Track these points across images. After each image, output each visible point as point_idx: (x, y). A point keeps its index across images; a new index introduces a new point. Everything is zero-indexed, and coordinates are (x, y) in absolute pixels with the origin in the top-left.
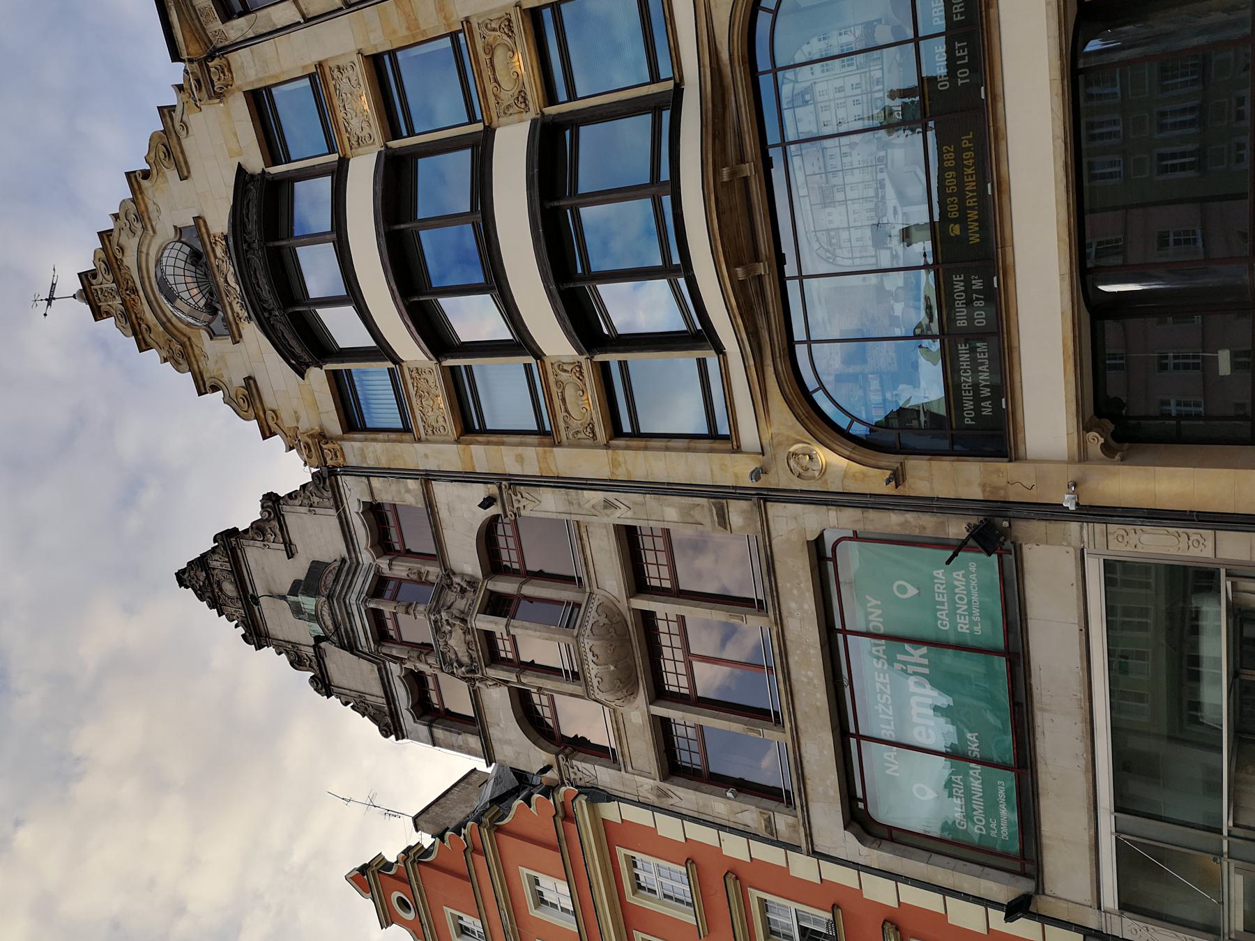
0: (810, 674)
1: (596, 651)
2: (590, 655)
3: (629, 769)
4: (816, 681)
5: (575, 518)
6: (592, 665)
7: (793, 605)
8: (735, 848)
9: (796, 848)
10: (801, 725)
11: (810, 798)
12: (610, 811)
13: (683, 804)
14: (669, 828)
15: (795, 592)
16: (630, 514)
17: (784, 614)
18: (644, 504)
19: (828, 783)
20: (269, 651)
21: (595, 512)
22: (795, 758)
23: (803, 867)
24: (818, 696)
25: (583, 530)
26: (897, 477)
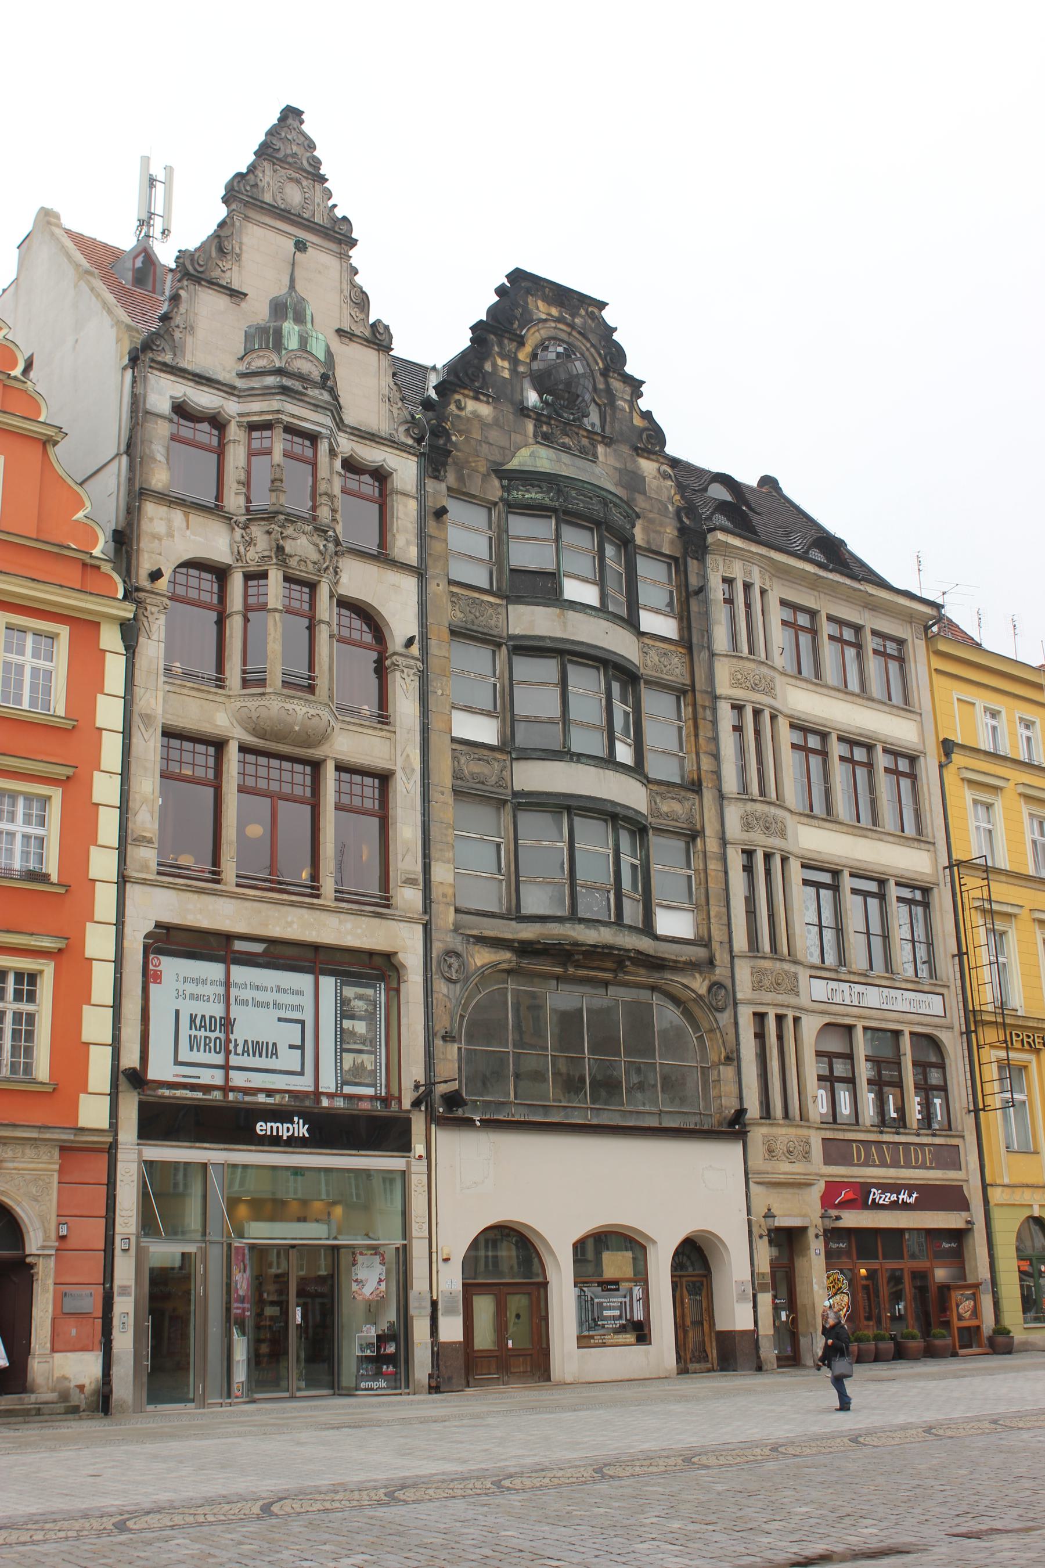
0: (295, 926)
1: (316, 719)
2: (312, 712)
4: (289, 929)
6: (304, 710)
7: (349, 926)
8: (105, 789)
10: (248, 904)
11: (180, 892)
14: (109, 712)
15: (359, 931)
17: (342, 916)
19: (199, 917)
20: (221, 212)
22: (221, 891)
23: (103, 864)
24: (278, 929)
25: (388, 734)
26: (448, 1038)
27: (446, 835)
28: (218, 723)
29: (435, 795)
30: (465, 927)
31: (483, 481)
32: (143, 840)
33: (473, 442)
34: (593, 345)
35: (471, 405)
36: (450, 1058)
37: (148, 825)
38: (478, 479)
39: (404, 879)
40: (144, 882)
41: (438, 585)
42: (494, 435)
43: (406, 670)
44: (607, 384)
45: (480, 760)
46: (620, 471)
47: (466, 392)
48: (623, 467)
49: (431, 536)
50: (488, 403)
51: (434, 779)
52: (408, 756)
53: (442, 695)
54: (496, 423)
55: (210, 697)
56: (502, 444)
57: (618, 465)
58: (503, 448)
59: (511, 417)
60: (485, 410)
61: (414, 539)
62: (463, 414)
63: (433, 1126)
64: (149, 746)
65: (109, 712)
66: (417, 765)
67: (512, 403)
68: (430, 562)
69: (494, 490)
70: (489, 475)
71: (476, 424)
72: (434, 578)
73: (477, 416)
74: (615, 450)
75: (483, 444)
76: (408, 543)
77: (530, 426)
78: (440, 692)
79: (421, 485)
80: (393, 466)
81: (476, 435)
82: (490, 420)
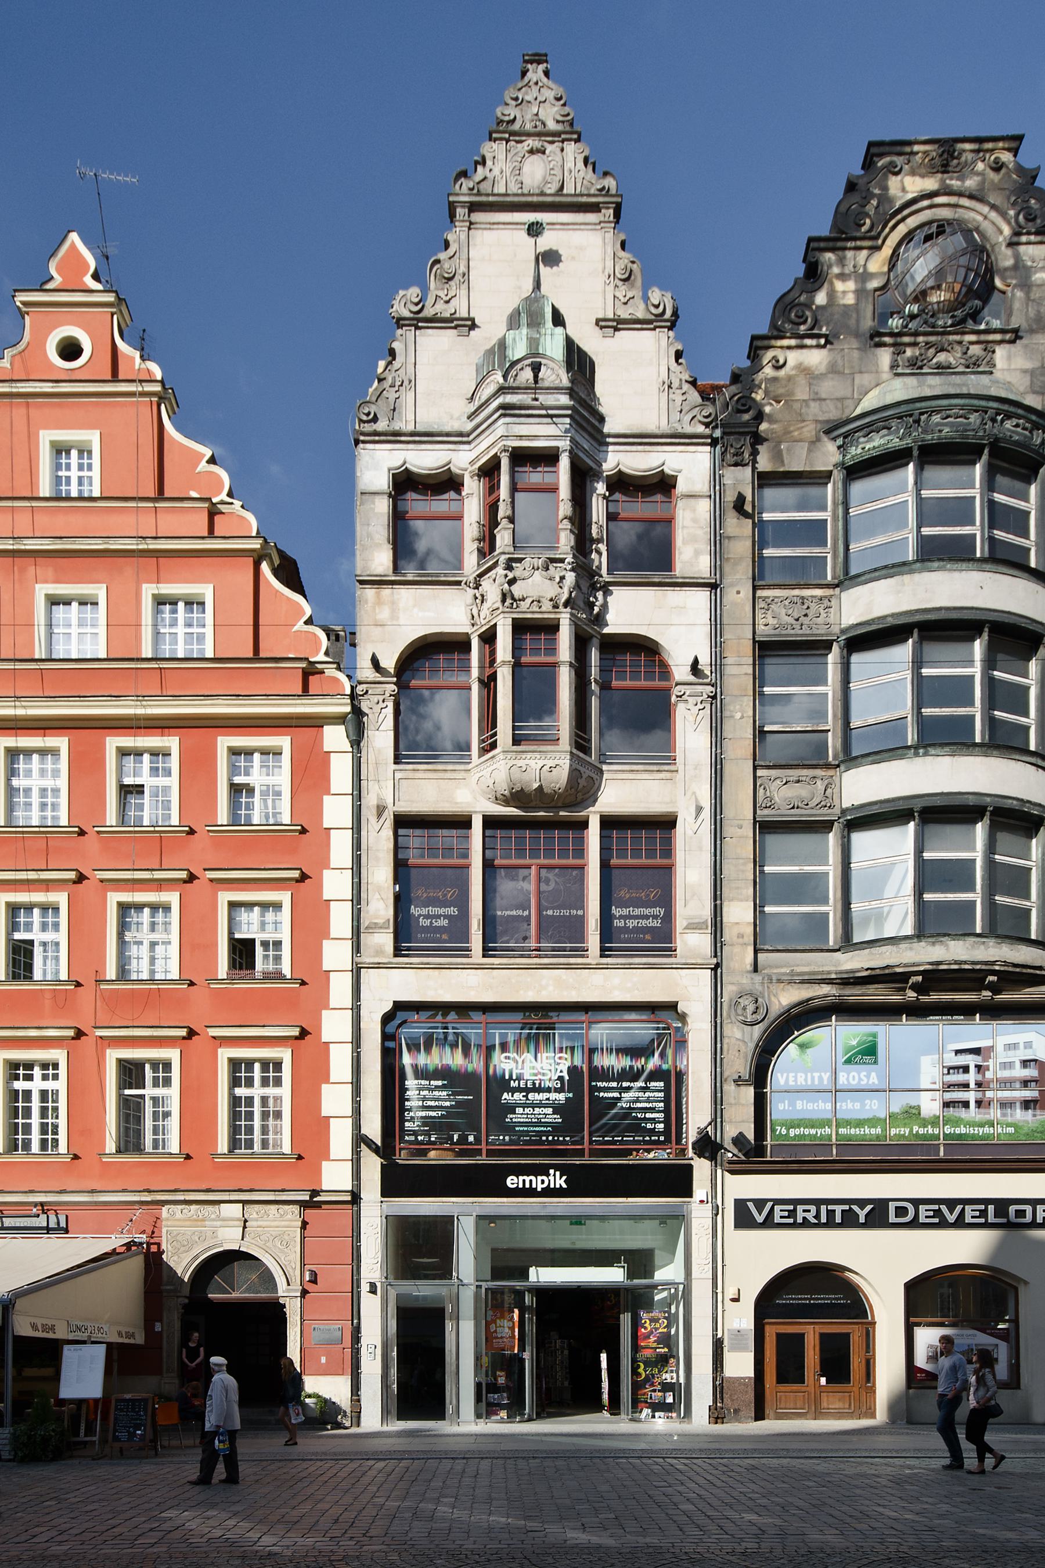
0: (551, 988)
3: (398, 775)
5: (681, 768)
8: (336, 884)
9: (357, 948)
12: (335, 737)
13: (373, 834)
14: (336, 811)
16: (690, 833)
18: (700, 849)
21: (689, 794)
23: (336, 955)
25: (668, 775)
27: (743, 871)
28: (459, 800)
29: (729, 830)
30: (770, 967)
31: (809, 451)
32: (374, 927)
33: (796, 406)
34: (993, 207)
35: (793, 358)
36: (743, 1102)
37: (382, 913)
38: (802, 450)
39: (685, 924)
40: (378, 966)
41: (738, 592)
42: (828, 387)
43: (690, 699)
44: (1017, 257)
45: (798, 781)
46: (1032, 373)
47: (785, 342)
48: (1037, 364)
49: (729, 538)
50: (818, 346)
51: (728, 812)
52: (694, 793)
53: (742, 717)
54: (833, 369)
55: (448, 775)
56: (839, 394)
57: (1029, 365)
58: (841, 400)
59: (856, 354)
60: (815, 358)
61: (705, 547)
62: (782, 373)
63: (719, 1171)
64: (380, 839)
65: (336, 811)
66: (706, 802)
67: (857, 335)
68: (727, 568)
69: (829, 455)
70: (818, 440)
71: (802, 381)
72: (732, 585)
73: (803, 370)
74: (1026, 346)
75: (812, 404)
76: (697, 553)
77: (885, 357)
78: (738, 715)
79: (716, 479)
80: (677, 468)
81: (801, 393)
82: (823, 369)
